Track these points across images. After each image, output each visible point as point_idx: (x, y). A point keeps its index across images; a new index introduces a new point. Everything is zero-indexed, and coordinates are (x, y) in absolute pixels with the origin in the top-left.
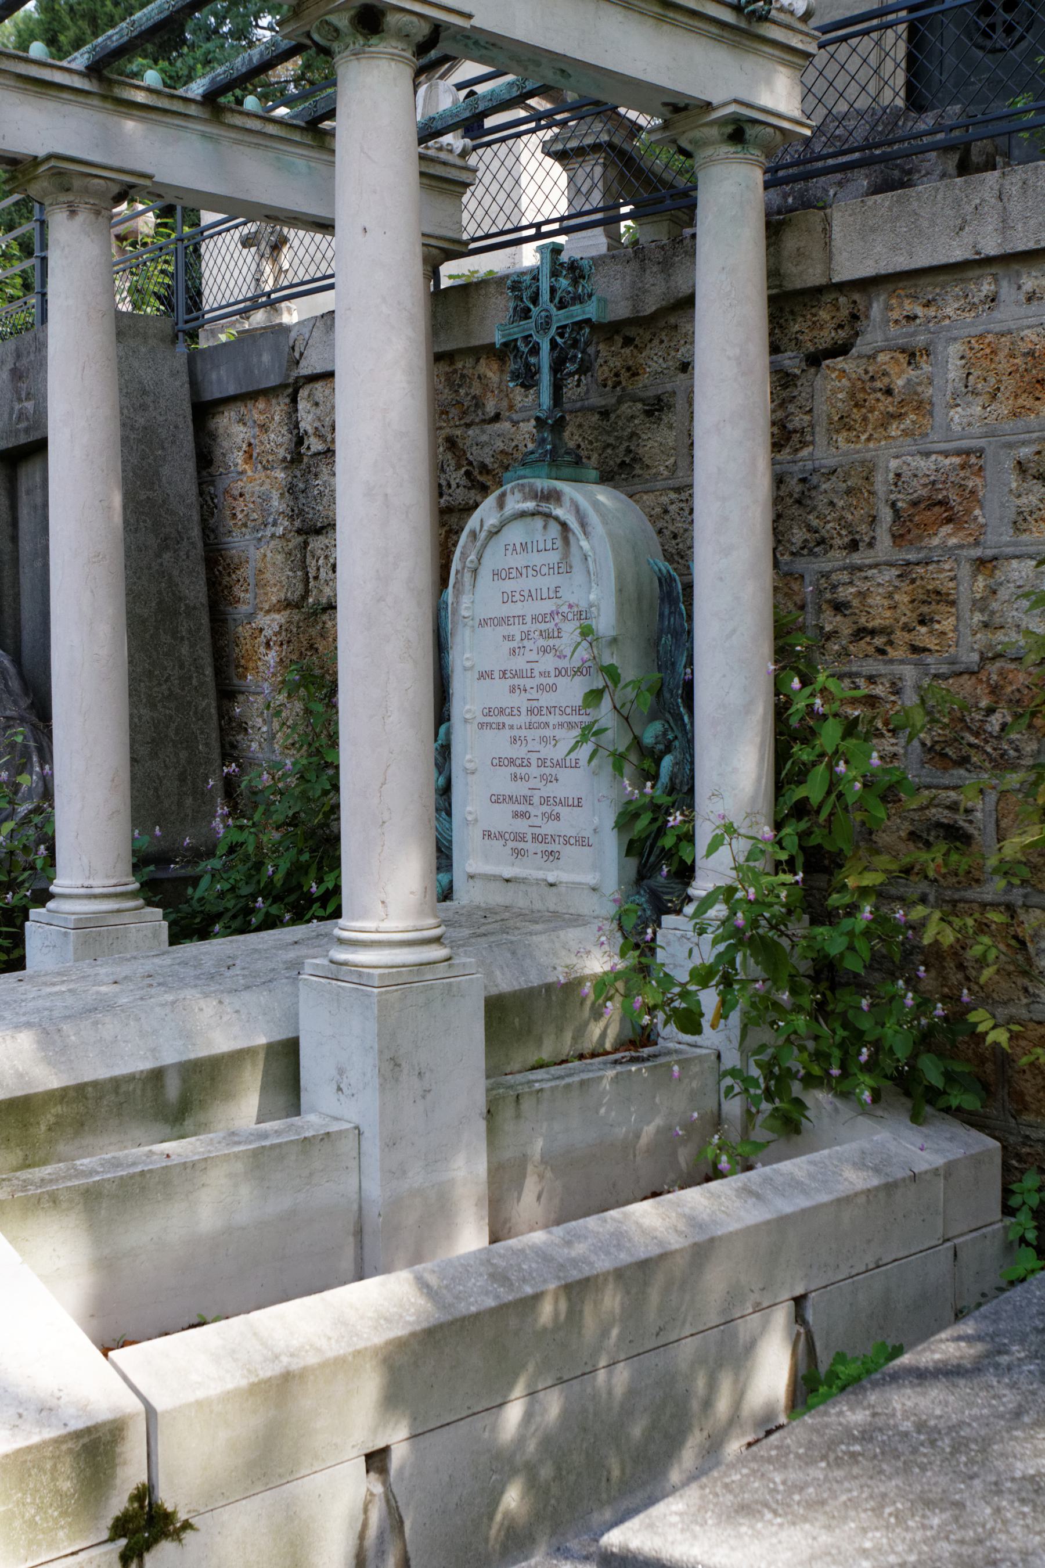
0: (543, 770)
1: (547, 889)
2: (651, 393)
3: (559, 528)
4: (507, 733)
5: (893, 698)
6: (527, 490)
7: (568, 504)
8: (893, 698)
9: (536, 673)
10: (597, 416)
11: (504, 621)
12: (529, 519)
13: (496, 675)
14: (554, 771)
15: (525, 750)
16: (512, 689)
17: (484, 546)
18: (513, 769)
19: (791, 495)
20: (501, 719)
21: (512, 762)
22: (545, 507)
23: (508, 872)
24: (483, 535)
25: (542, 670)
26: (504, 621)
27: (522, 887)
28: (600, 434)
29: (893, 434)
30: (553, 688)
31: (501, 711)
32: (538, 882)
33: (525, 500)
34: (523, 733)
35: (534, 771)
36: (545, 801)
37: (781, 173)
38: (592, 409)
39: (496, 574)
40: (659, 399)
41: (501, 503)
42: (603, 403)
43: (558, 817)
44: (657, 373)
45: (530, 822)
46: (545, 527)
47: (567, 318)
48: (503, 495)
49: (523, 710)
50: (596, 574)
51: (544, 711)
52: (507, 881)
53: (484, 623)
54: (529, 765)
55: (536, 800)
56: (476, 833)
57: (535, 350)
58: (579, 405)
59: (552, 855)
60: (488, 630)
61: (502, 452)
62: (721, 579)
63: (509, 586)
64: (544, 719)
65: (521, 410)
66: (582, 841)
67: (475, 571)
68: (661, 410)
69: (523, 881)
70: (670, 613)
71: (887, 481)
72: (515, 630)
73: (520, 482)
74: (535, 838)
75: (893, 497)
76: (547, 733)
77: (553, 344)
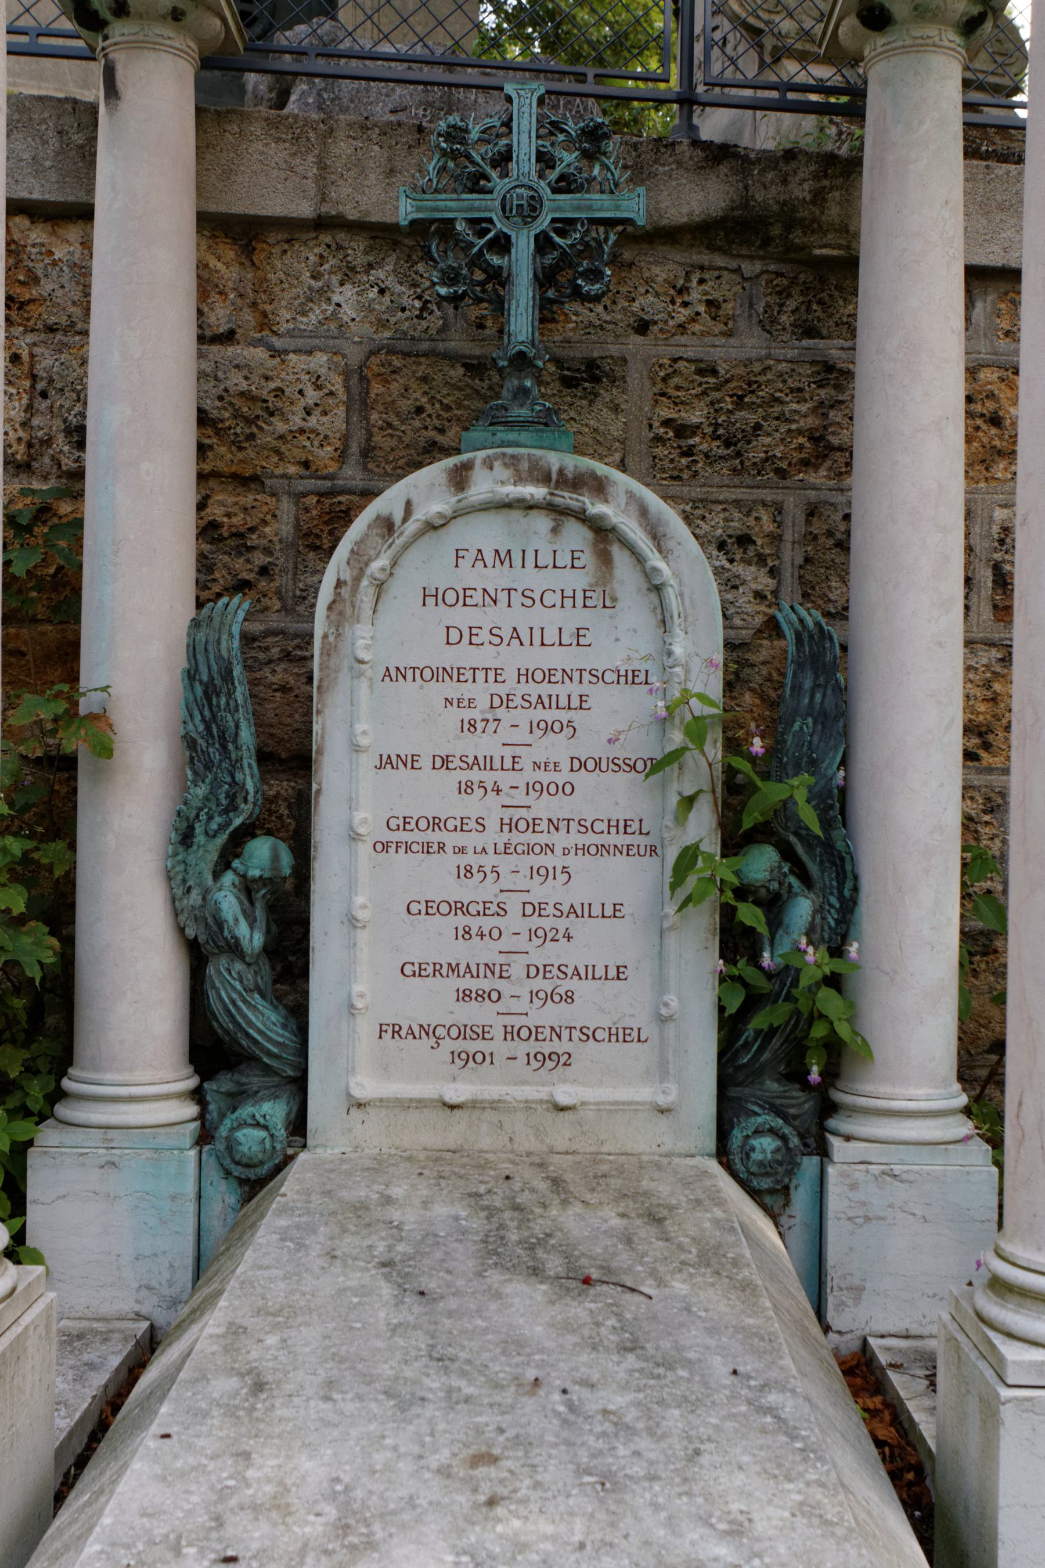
0: (535, 921)
1: (551, 1116)
2: (578, 352)
3: (589, 535)
4: (451, 861)
5: (987, 818)
6: (525, 465)
7: (623, 500)
8: (987, 818)
9: (526, 763)
10: (461, 371)
11: (453, 674)
12: (516, 514)
13: (425, 762)
14: (562, 924)
15: (496, 888)
16: (465, 789)
17: (406, 547)
18: (462, 920)
19: (830, 534)
20: (435, 837)
21: (460, 908)
22: (567, 498)
23: (454, 1093)
24: (411, 527)
25: (541, 759)
26: (453, 674)
27: (490, 1115)
28: (467, 397)
29: (999, 475)
30: (567, 789)
31: (435, 823)
32: (528, 1106)
33: (519, 480)
34: (489, 860)
35: (513, 921)
36: (534, 971)
37: (791, 96)
38: (452, 358)
39: (431, 596)
40: (591, 365)
41: (460, 478)
42: (477, 352)
43: (569, 997)
44: (591, 324)
45: (500, 1007)
46: (555, 531)
47: (578, 208)
48: (467, 467)
49: (492, 824)
50: (684, 615)
51: (544, 826)
52: (452, 1107)
53: (395, 674)
54: (502, 910)
55: (517, 970)
56: (365, 1028)
57: (502, 244)
58: (425, 346)
59: (562, 1061)
60: (408, 688)
61: (242, 394)
62: (940, 645)
63: (462, 617)
64: (543, 839)
65: (290, 334)
66: (621, 1035)
67: (380, 587)
68: (596, 380)
69: (494, 1105)
70: (816, 686)
71: (989, 534)
72: (480, 692)
73: (509, 451)
74: (511, 1033)
75: (997, 556)
76: (547, 860)
77: (543, 244)
